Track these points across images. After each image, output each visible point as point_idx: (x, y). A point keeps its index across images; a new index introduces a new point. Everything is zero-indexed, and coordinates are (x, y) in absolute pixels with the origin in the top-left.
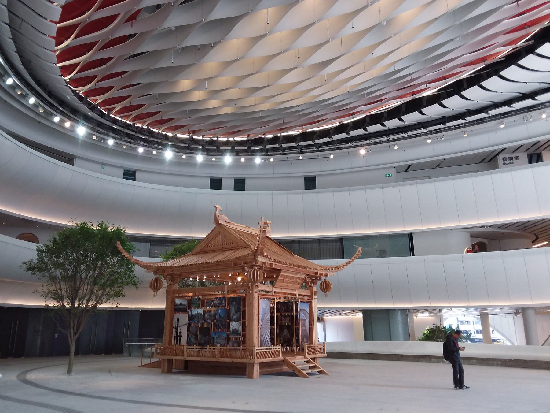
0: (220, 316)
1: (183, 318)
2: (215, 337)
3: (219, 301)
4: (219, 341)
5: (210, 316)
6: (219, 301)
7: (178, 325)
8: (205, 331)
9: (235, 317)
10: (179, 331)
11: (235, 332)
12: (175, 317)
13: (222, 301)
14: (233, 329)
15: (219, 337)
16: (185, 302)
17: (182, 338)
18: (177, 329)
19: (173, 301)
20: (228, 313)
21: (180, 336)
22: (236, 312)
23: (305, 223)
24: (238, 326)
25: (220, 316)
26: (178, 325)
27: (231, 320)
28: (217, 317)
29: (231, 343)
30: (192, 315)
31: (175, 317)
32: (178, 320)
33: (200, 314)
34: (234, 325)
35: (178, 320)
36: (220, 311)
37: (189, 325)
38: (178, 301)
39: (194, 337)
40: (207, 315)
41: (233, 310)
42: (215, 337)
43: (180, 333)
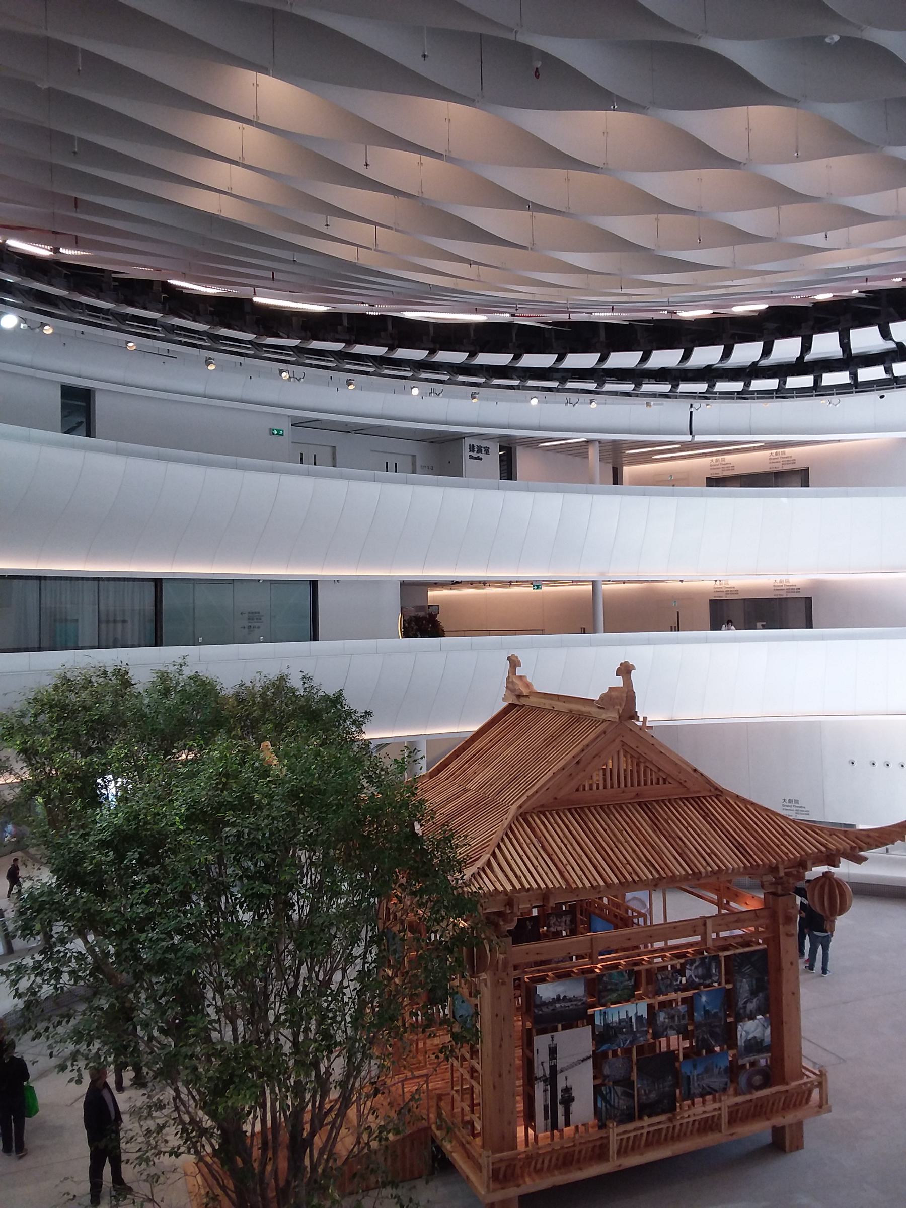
0: (707, 1012)
1: (576, 1043)
2: (695, 1073)
3: (700, 971)
4: (706, 1081)
5: (672, 1018)
6: (700, 971)
7: (553, 1069)
8: (658, 1065)
9: (751, 1006)
10: (561, 1084)
11: (755, 1046)
12: (541, 1042)
13: (709, 969)
14: (748, 1041)
15: (707, 1070)
16: (575, 990)
17: (574, 1107)
18: (551, 1079)
19: (530, 993)
20: (729, 999)
21: (568, 1100)
22: (754, 993)
23: (97, 538)
24: (760, 1029)
25: (707, 1012)
26: (553, 1069)
27: (739, 1018)
28: (698, 1016)
29: (743, 1079)
30: (607, 1026)
31: (541, 1042)
32: (553, 1052)
33: (639, 1018)
34: (752, 1029)
35: (553, 1052)
36: (704, 999)
37: (598, 1059)
38: (546, 991)
39: (619, 1089)
40: (662, 1017)
41: (745, 986)
42: (695, 1073)
43: (567, 1090)
